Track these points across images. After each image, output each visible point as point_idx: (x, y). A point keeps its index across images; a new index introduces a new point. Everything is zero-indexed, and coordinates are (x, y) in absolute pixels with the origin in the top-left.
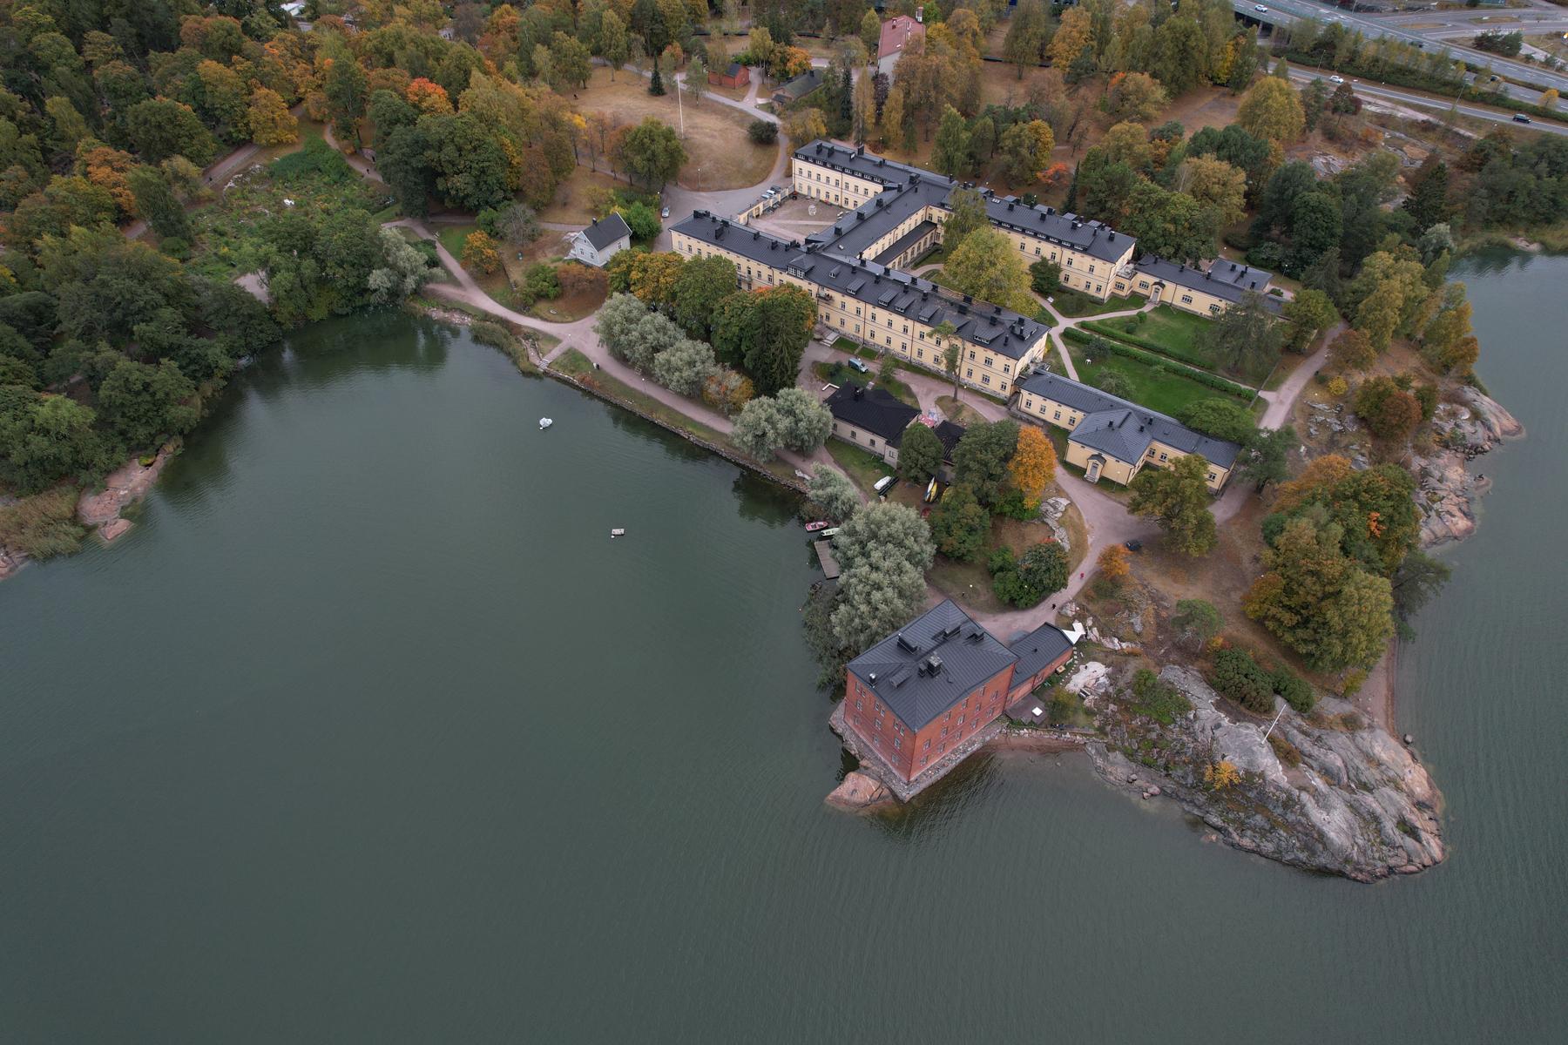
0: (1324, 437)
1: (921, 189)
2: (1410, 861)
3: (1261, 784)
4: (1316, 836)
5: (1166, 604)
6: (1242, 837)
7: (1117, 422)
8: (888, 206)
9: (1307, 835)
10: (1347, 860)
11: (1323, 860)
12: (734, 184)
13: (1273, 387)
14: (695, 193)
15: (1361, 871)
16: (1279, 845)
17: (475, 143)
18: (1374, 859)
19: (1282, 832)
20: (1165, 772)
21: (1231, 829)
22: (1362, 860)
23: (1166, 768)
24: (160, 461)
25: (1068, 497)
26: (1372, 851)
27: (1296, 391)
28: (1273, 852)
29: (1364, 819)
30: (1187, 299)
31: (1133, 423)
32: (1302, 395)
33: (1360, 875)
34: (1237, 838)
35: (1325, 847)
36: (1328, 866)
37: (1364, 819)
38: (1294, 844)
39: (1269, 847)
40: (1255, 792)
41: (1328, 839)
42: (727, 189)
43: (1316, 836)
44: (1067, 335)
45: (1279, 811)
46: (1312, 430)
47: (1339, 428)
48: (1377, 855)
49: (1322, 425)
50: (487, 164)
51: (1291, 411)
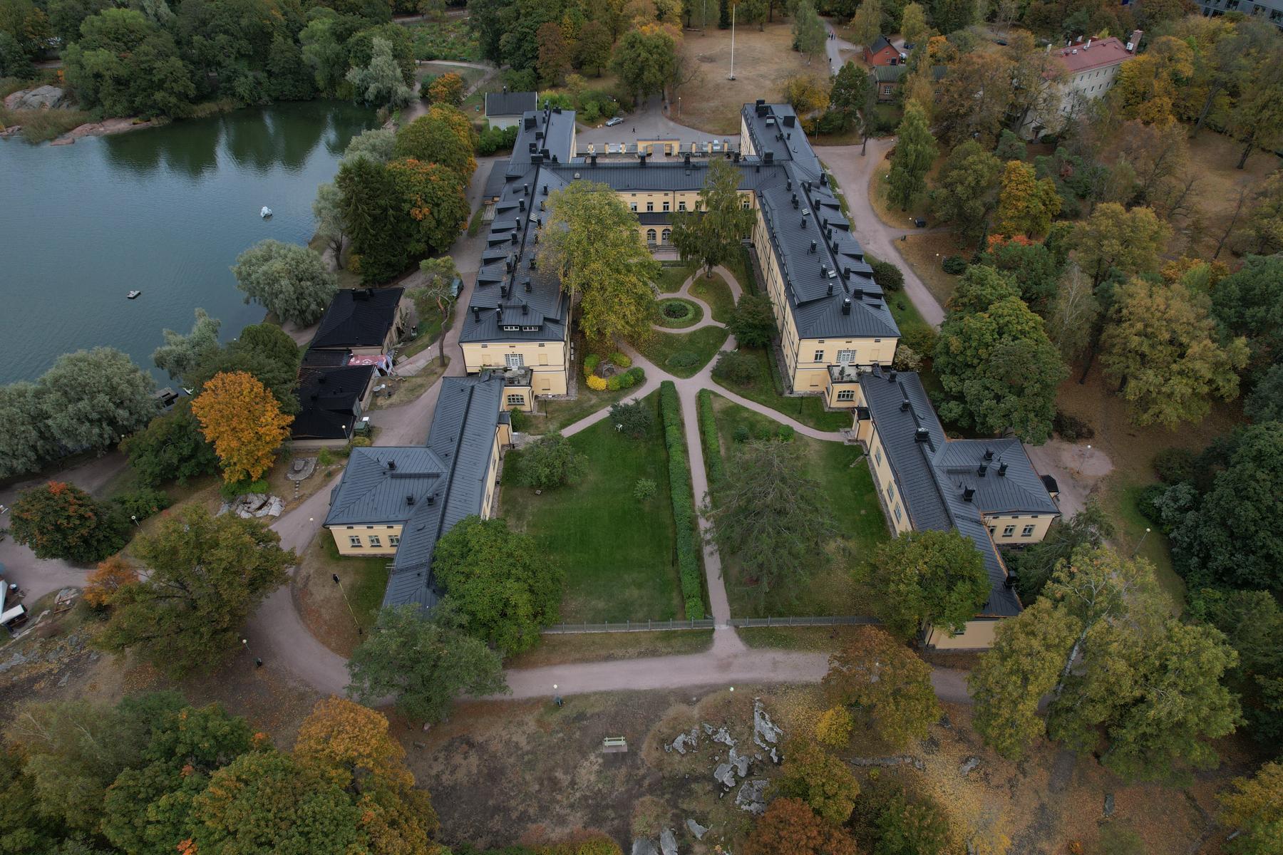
0: (681, 766)
1: (766, 173)
5: (64, 679)
7: (399, 471)
8: (696, 168)
12: (709, 127)
13: (751, 638)
14: (666, 120)
17: (530, 9)
24: (142, 125)
25: (284, 513)
27: (781, 676)
30: (878, 458)
31: (421, 489)
32: (771, 688)
42: (697, 129)
44: (665, 399)
46: (681, 738)
47: (726, 778)
49: (713, 751)
50: (527, 30)
51: (713, 689)
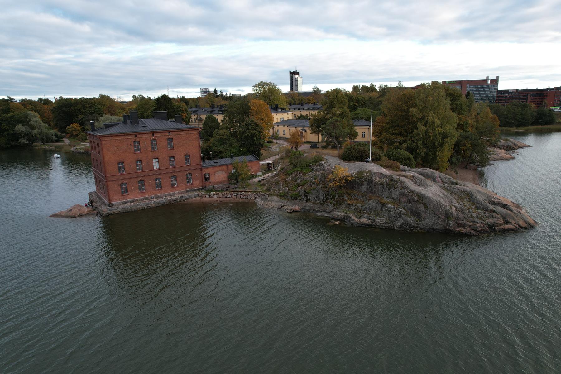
2: (506, 222)
3: (368, 176)
4: (416, 199)
6: (361, 217)
9: (409, 202)
10: (448, 216)
11: (428, 222)
15: (463, 226)
16: (390, 217)
18: (472, 217)
19: (390, 205)
20: (305, 199)
21: (351, 215)
22: (461, 216)
23: (306, 196)
26: (469, 212)
28: (386, 223)
29: (458, 196)
33: (463, 229)
34: (356, 220)
35: (426, 207)
36: (434, 227)
37: (458, 196)
38: (401, 211)
39: (381, 220)
40: (365, 183)
41: (426, 198)
43: (416, 199)
45: (386, 193)
48: (474, 215)
